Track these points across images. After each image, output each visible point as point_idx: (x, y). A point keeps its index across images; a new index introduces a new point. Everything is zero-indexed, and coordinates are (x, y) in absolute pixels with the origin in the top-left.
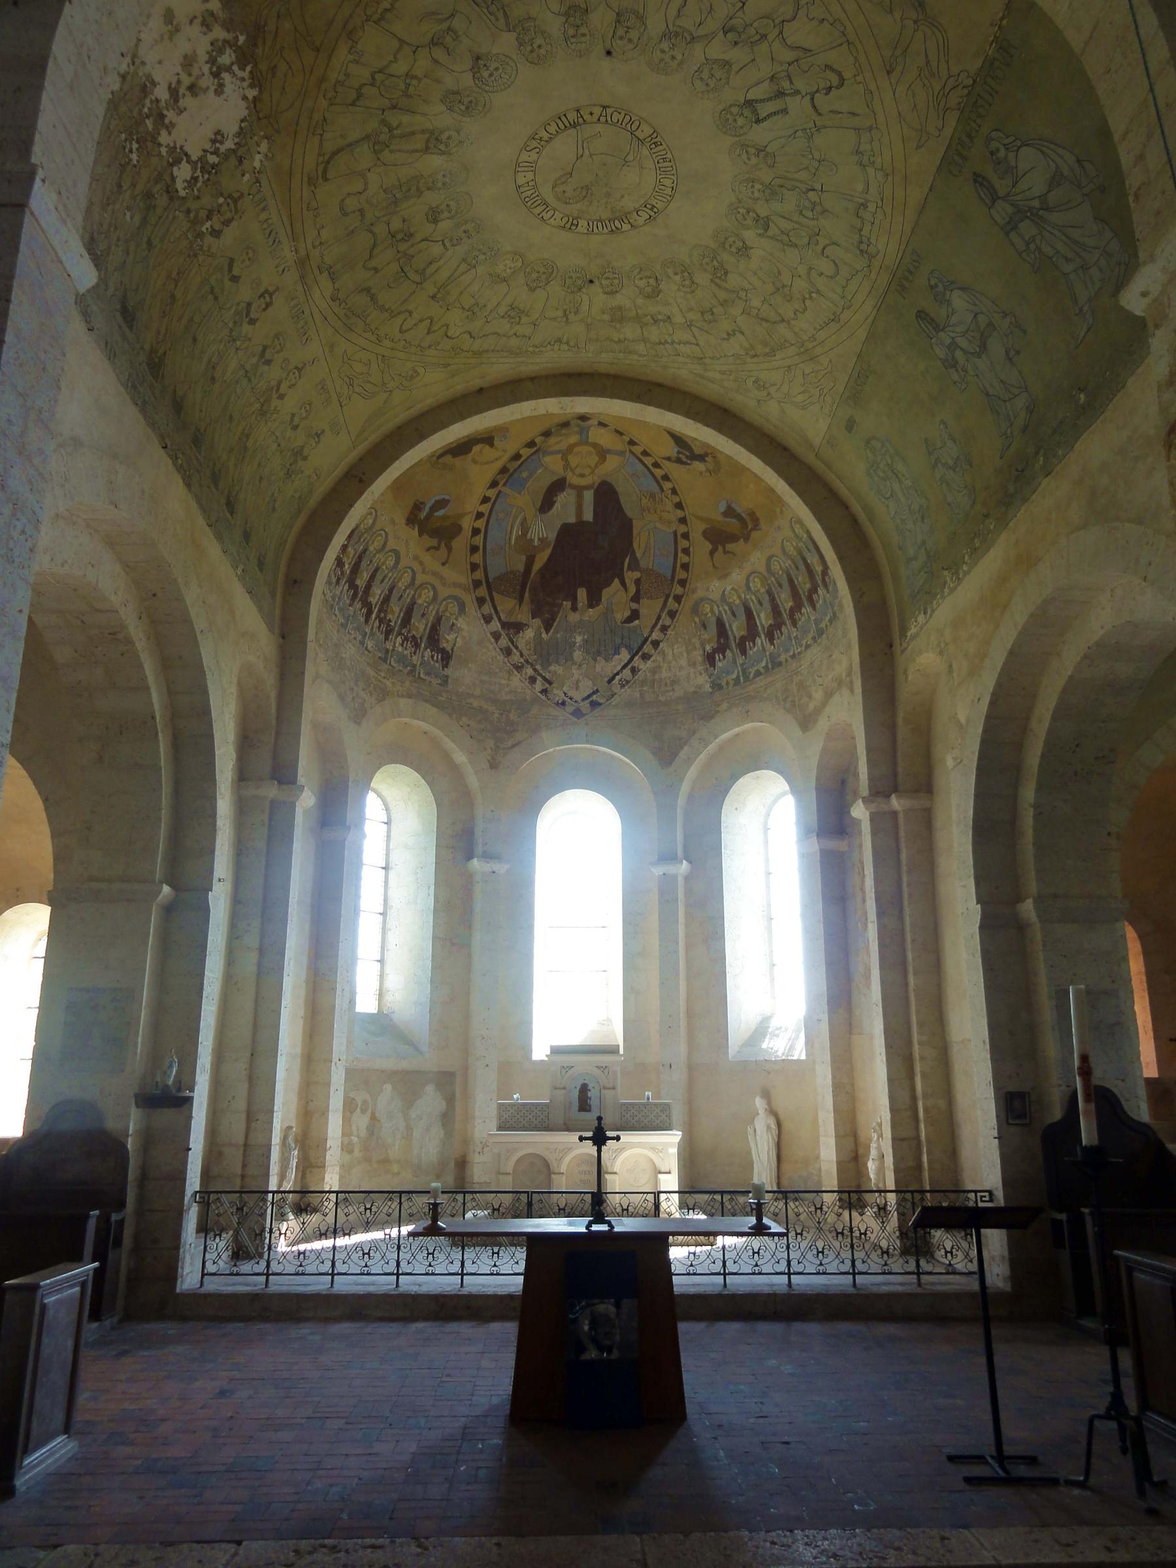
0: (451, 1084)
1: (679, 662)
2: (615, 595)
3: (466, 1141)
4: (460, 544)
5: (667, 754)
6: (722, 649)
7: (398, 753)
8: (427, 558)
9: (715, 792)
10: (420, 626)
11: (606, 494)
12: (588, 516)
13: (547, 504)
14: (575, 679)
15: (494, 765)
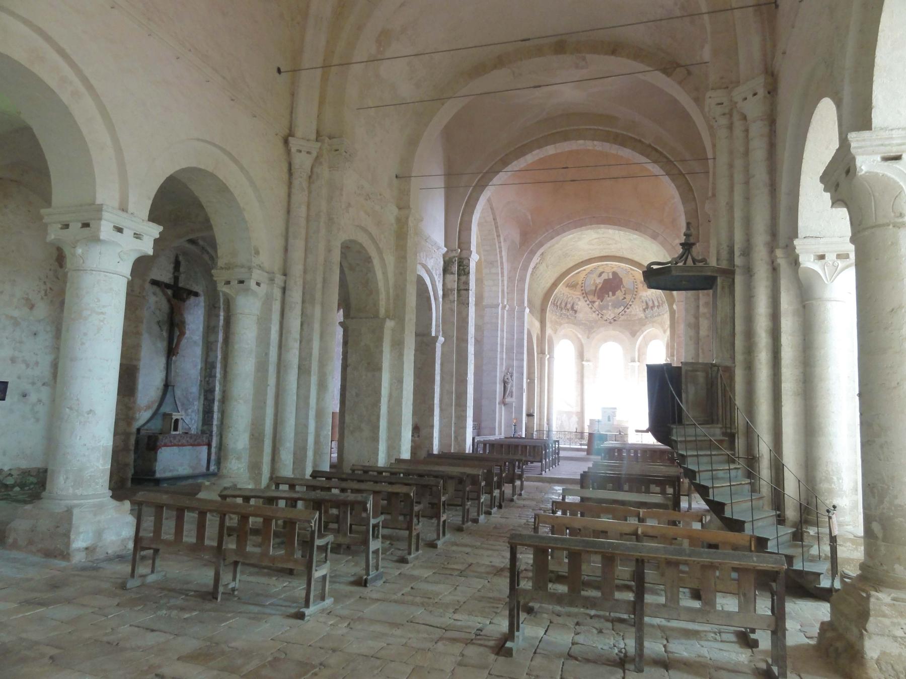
0: (581, 415)
1: (636, 310)
2: (619, 293)
3: (583, 428)
4: (579, 286)
5: (634, 334)
6: (647, 308)
7: (566, 336)
8: (571, 292)
9: (646, 343)
10: (569, 306)
11: (615, 274)
12: (611, 277)
13: (600, 275)
14: (610, 314)
15: (588, 337)
